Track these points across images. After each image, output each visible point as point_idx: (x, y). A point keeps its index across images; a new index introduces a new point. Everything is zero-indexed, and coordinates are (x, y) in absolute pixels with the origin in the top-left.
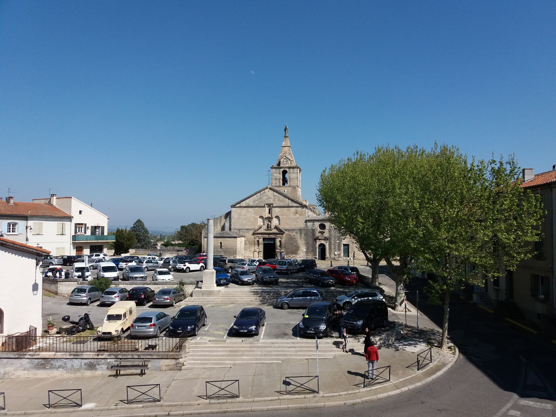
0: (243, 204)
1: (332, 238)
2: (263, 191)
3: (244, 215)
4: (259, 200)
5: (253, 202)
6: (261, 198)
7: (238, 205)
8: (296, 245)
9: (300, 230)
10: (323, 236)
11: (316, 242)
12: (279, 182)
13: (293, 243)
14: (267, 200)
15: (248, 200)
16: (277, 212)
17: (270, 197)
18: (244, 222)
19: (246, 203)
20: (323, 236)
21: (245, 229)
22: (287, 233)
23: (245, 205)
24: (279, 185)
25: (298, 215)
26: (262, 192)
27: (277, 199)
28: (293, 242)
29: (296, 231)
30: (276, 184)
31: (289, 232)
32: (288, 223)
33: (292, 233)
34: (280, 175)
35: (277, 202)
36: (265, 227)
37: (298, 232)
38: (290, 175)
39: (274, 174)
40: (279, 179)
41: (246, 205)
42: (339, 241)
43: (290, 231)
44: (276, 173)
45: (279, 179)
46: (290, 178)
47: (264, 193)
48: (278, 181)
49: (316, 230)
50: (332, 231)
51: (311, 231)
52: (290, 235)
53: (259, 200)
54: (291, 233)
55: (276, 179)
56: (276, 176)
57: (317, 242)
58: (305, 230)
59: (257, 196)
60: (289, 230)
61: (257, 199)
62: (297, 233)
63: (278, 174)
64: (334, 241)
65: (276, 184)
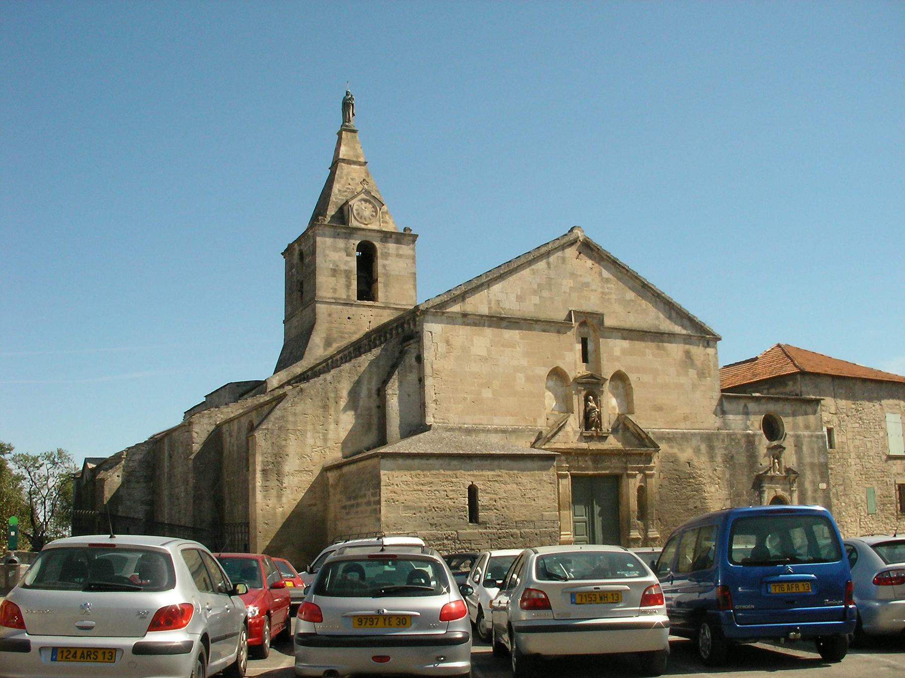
0: (479, 304)
1: (804, 474)
2: (560, 254)
3: (484, 359)
4: (545, 294)
5: (520, 298)
6: (550, 285)
7: (456, 308)
8: (698, 504)
9: (709, 439)
10: (779, 463)
11: (761, 493)
12: (348, 286)
13: (689, 498)
14: (574, 296)
15: (497, 288)
16: (617, 352)
17: (587, 285)
18: (487, 394)
19: (489, 302)
20: (779, 463)
21: (496, 431)
22: (663, 446)
23: (484, 310)
24: (348, 296)
25: (692, 373)
26: (552, 259)
27: (613, 297)
28: (688, 492)
29: (694, 443)
30: (335, 290)
31: (672, 447)
32: (659, 409)
33: (682, 450)
34: (348, 259)
35: (618, 308)
36: (574, 423)
37: (703, 447)
38: (386, 262)
39: (327, 252)
40: (347, 273)
41: (490, 308)
42: (823, 486)
43: (674, 444)
44: (335, 249)
45: (347, 273)
46: (387, 275)
47: (564, 260)
48: (342, 281)
49: (757, 439)
50: (802, 444)
51: (743, 441)
52: (675, 460)
53: (545, 294)
54: (678, 449)
55: (335, 272)
56: (334, 263)
57: (764, 491)
58: (723, 441)
59: (534, 272)
60: (669, 439)
61: (535, 287)
62: (697, 451)
63: (343, 254)
64: (813, 483)
65: (335, 290)
